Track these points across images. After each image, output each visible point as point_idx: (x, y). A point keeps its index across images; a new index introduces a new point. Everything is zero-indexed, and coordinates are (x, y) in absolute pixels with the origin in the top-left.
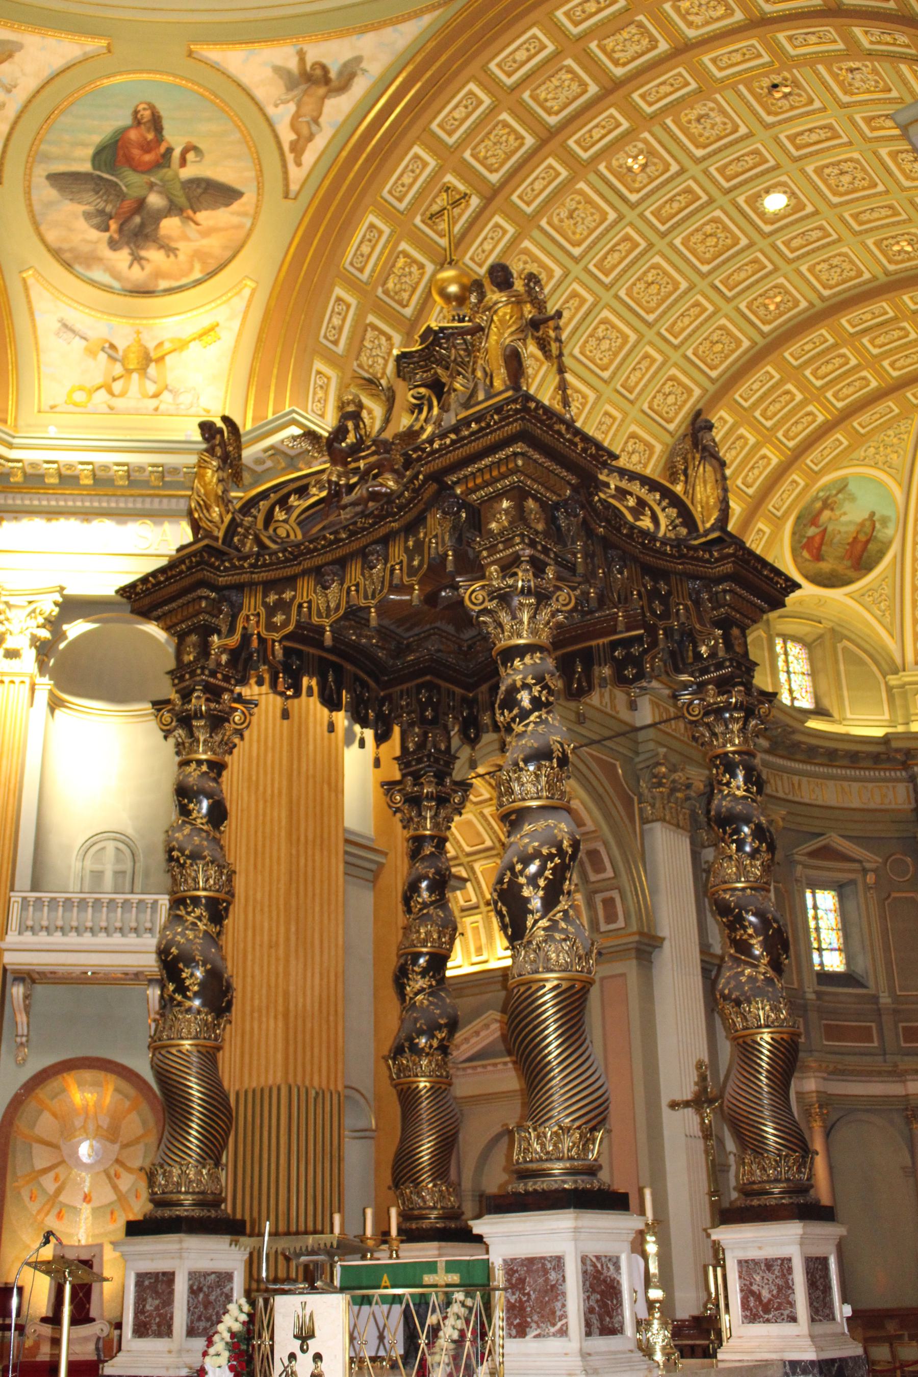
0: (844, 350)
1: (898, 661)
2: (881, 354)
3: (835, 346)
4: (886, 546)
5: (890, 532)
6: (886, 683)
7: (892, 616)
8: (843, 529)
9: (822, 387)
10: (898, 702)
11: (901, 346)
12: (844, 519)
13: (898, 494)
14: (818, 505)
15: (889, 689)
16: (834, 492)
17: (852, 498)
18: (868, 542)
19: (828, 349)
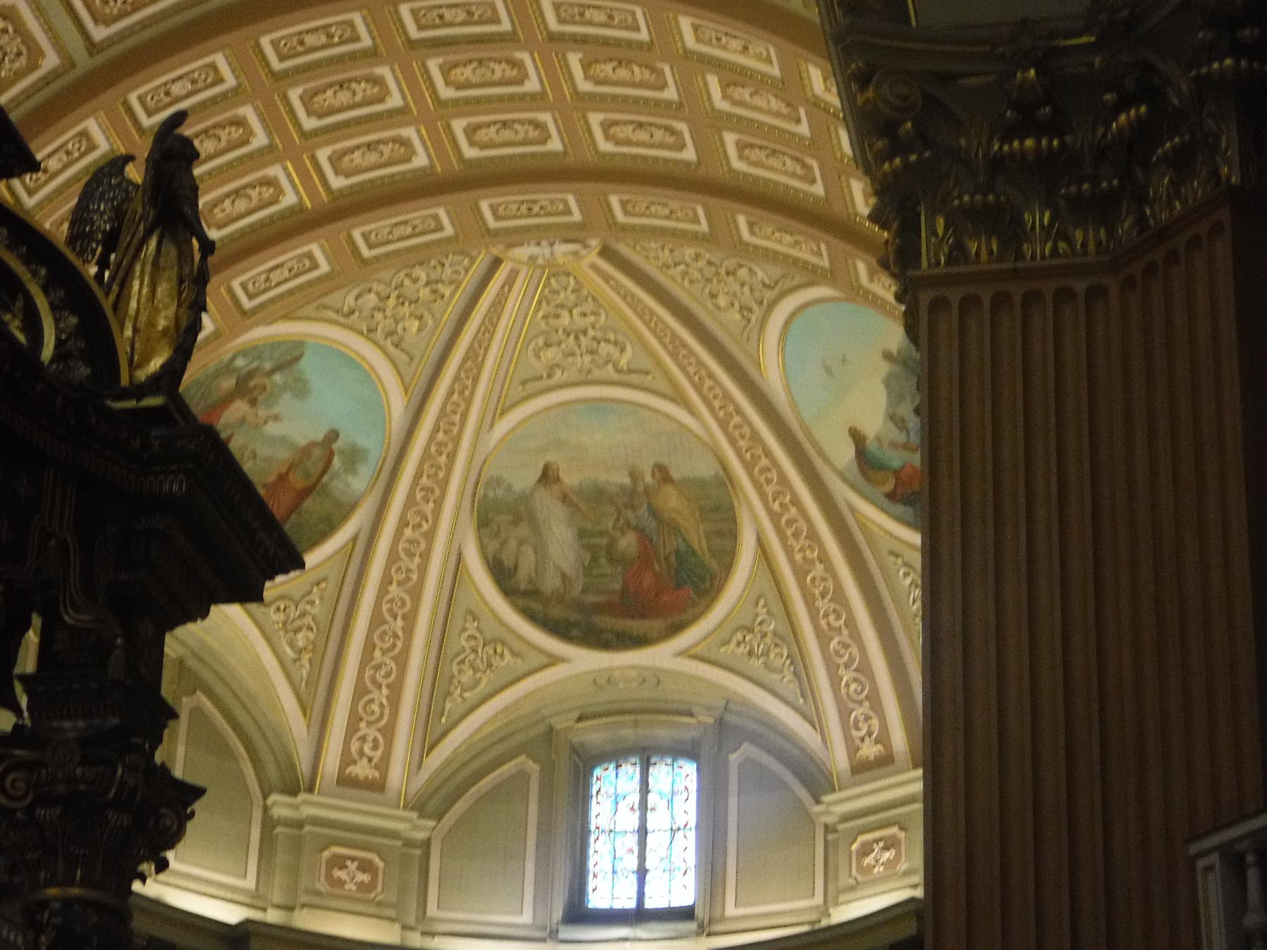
0: (384, 71)
1: (304, 766)
2: (456, 102)
3: (371, 55)
4: (345, 511)
5: (358, 482)
6: (266, 809)
7: (316, 665)
8: (264, 451)
9: (316, 133)
10: (281, 857)
11: (501, 98)
12: (272, 429)
13: (398, 404)
14: (228, 383)
15: (269, 824)
16: (268, 366)
17: (301, 389)
18: (306, 492)
19: (353, 56)
